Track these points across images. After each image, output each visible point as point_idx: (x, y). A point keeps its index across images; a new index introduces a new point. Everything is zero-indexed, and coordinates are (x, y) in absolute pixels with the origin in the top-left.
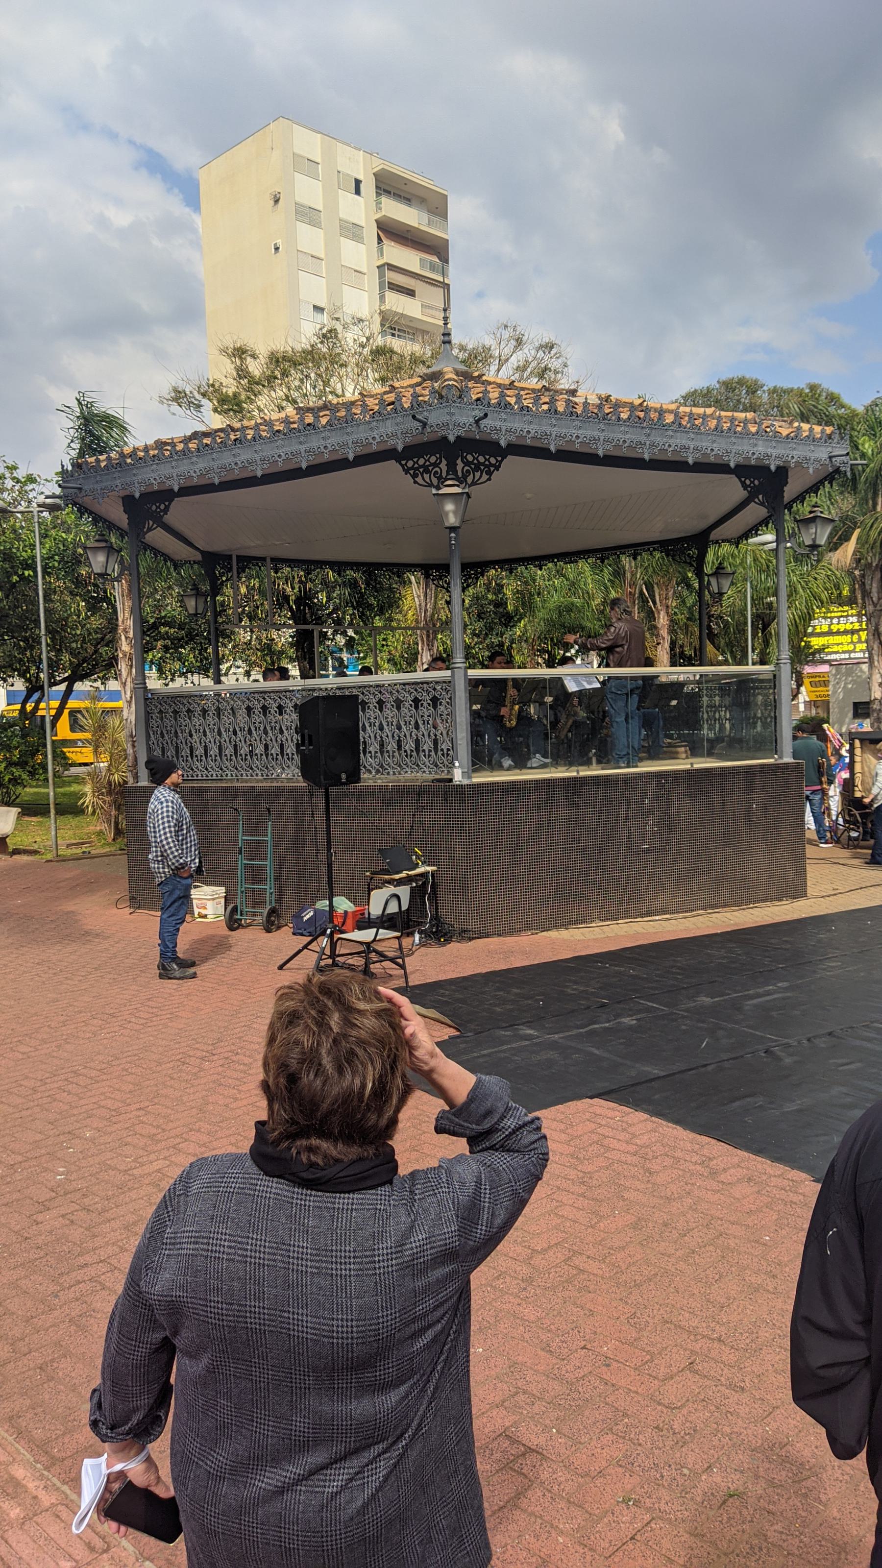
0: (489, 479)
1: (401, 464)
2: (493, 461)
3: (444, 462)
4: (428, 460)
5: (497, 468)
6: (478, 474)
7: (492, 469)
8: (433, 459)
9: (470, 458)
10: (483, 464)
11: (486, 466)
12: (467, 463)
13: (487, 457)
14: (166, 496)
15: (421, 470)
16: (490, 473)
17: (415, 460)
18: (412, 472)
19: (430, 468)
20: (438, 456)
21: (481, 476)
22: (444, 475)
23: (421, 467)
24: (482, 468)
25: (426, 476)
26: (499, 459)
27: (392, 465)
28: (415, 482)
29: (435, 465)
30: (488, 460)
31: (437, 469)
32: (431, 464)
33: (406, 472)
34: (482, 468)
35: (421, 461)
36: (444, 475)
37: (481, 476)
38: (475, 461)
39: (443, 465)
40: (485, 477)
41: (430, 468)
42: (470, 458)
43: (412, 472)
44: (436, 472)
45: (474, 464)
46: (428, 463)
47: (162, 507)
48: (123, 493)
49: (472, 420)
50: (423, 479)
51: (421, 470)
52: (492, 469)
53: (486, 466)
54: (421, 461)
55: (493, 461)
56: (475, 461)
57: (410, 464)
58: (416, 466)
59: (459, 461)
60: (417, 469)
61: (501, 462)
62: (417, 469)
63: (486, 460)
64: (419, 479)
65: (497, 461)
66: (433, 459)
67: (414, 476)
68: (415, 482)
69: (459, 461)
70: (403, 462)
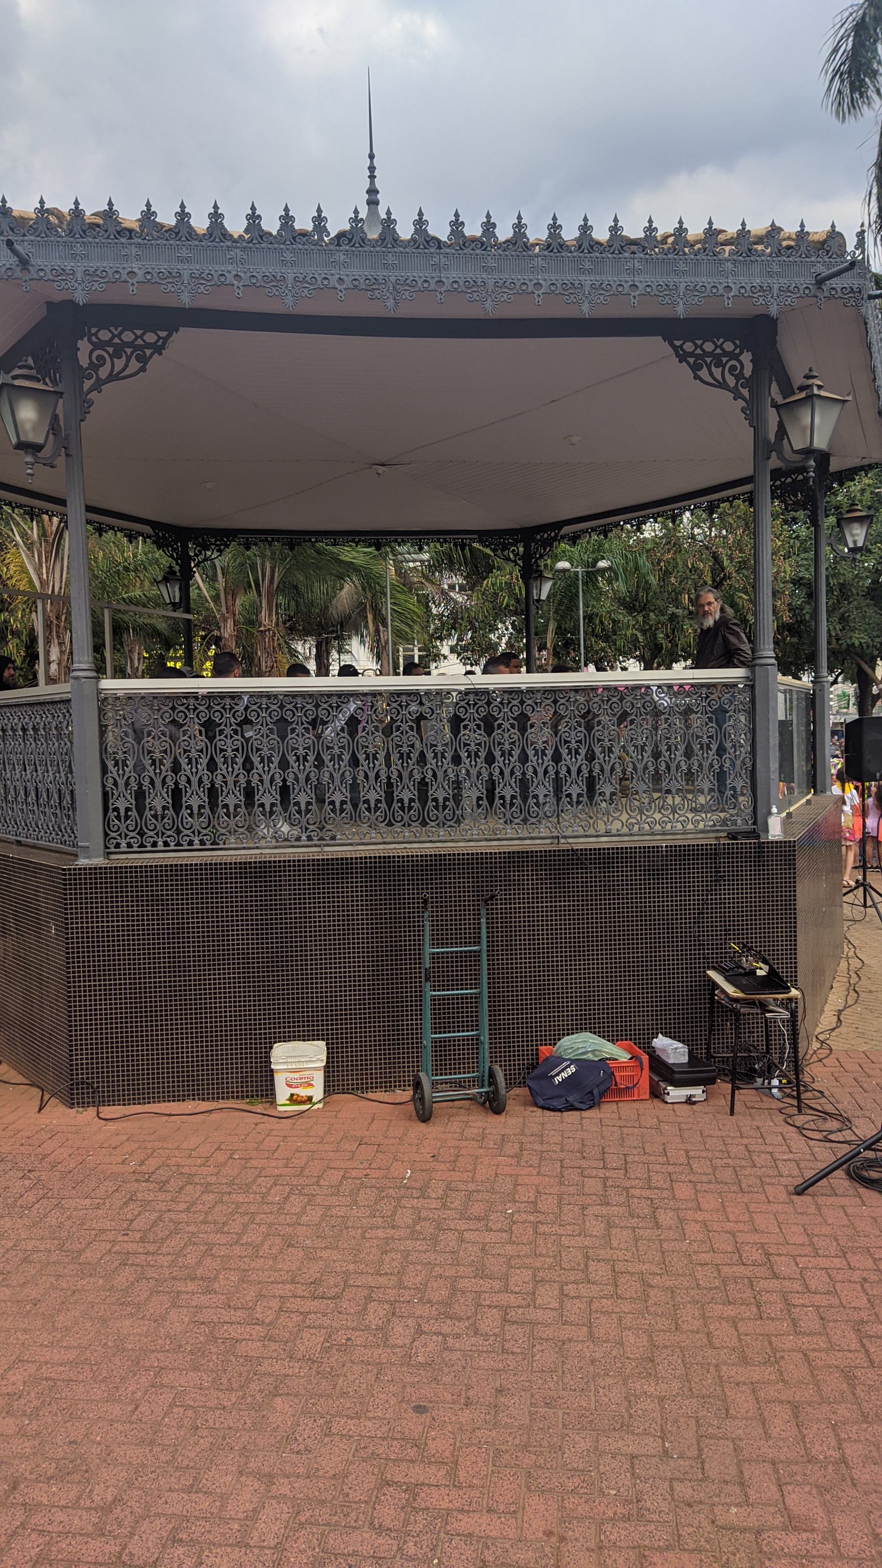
15: (708, 360)
18: (691, 360)
19: (724, 360)
25: (717, 372)
27: (656, 345)
28: (697, 377)
29: (732, 356)
33: (682, 357)
39: (746, 358)
41: (724, 360)
43: (691, 360)
46: (718, 351)
50: (711, 374)
57: (689, 347)
64: (704, 373)
67: (695, 368)
70: (678, 343)
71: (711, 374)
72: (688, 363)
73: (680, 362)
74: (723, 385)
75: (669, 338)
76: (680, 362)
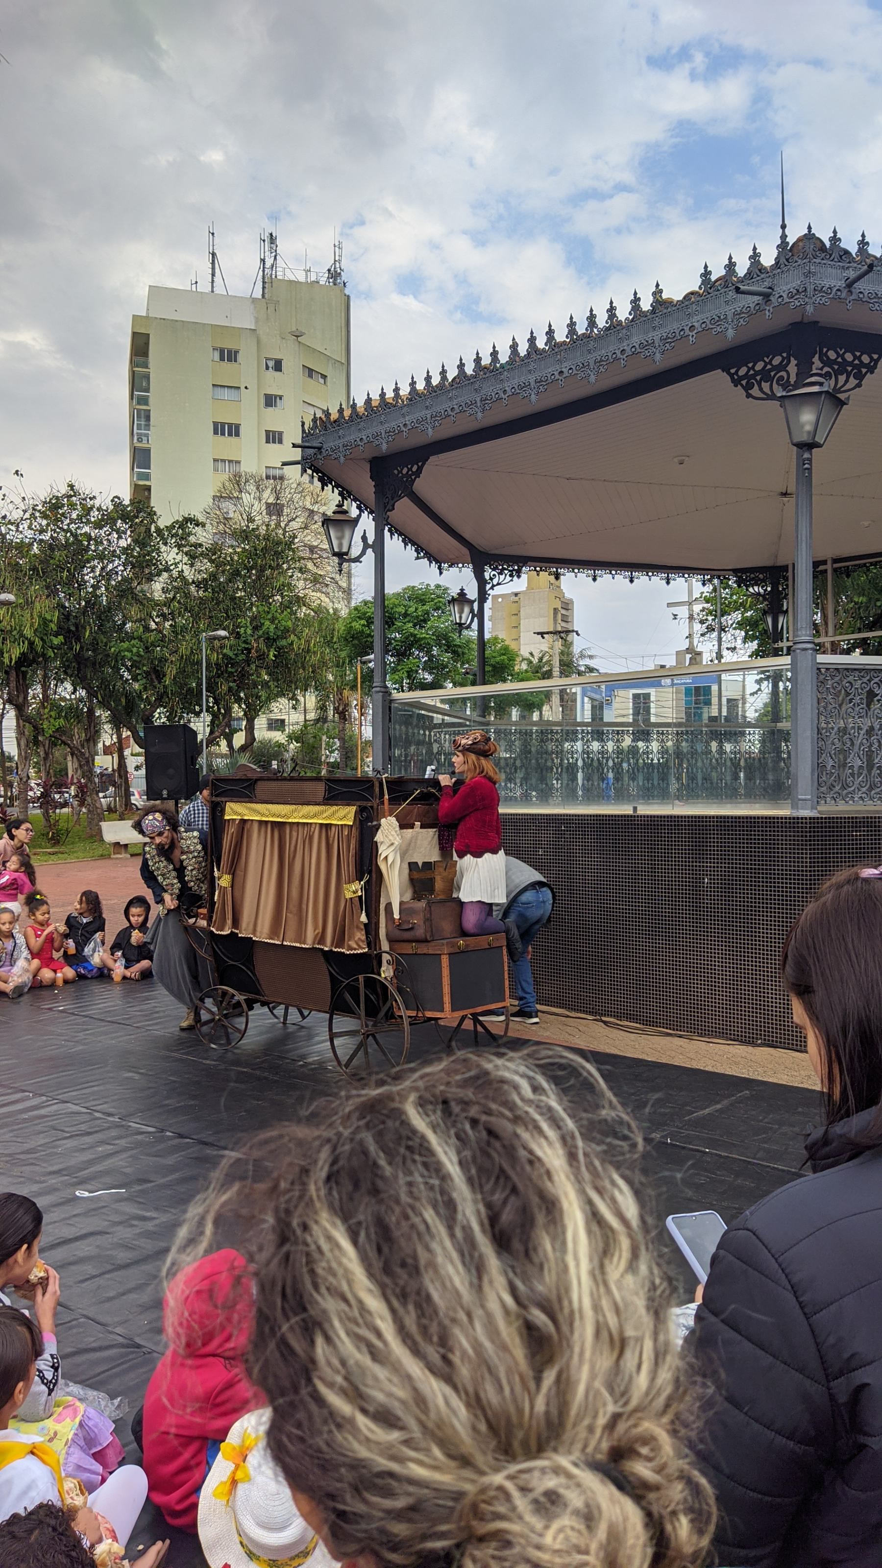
0: (859, 385)
1: (729, 373)
2: (866, 359)
3: (793, 362)
4: (770, 363)
5: (871, 369)
6: (842, 378)
7: (864, 370)
8: (777, 361)
9: (832, 355)
10: (851, 364)
11: (854, 367)
12: (827, 362)
13: (858, 354)
14: (420, 454)
16: (860, 377)
17: (750, 365)
18: (744, 382)
20: (785, 355)
21: (847, 381)
22: (793, 379)
23: (757, 373)
24: (849, 369)
25: (766, 386)
26: (875, 356)
27: (718, 378)
28: (749, 396)
30: (859, 358)
31: (783, 374)
32: (774, 368)
33: (736, 382)
34: (849, 369)
35: (759, 366)
36: (793, 379)
37: (847, 381)
38: (840, 360)
39: (792, 368)
40: (853, 382)
42: (832, 355)
43: (744, 382)
44: (782, 378)
45: (838, 363)
47: (415, 468)
48: (369, 455)
49: (841, 284)
50: (761, 389)
51: (758, 378)
52: (864, 370)
53: (854, 367)
54: (759, 366)
55: (866, 359)
56: (840, 360)
57: (743, 371)
58: (752, 372)
59: (816, 359)
60: (754, 377)
61: (876, 361)
62: (754, 377)
63: (855, 357)
64: (755, 391)
65: (872, 359)
66: (777, 361)
67: (748, 388)
68: (749, 396)
69: (816, 359)
70: (733, 371)
71: (761, 389)
72: (742, 385)
73: (736, 386)
74: (772, 397)
75: (726, 370)
76: (736, 386)
